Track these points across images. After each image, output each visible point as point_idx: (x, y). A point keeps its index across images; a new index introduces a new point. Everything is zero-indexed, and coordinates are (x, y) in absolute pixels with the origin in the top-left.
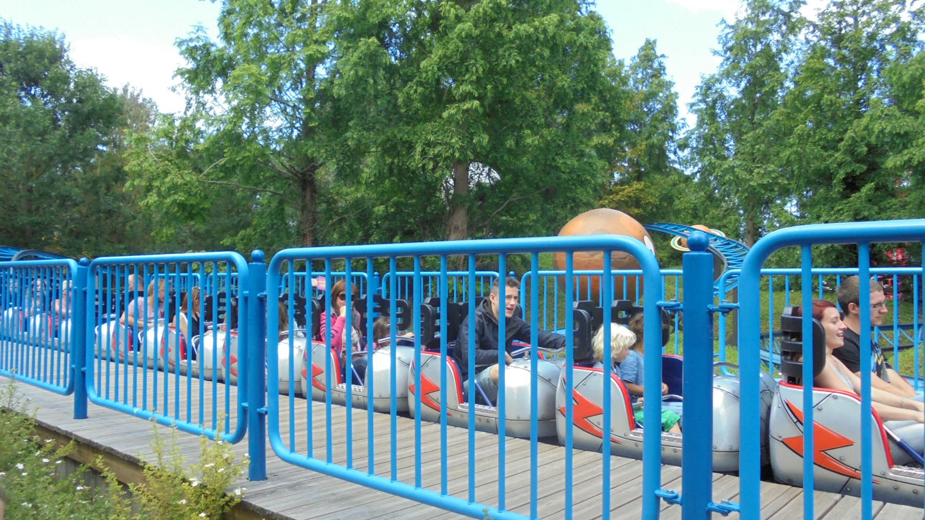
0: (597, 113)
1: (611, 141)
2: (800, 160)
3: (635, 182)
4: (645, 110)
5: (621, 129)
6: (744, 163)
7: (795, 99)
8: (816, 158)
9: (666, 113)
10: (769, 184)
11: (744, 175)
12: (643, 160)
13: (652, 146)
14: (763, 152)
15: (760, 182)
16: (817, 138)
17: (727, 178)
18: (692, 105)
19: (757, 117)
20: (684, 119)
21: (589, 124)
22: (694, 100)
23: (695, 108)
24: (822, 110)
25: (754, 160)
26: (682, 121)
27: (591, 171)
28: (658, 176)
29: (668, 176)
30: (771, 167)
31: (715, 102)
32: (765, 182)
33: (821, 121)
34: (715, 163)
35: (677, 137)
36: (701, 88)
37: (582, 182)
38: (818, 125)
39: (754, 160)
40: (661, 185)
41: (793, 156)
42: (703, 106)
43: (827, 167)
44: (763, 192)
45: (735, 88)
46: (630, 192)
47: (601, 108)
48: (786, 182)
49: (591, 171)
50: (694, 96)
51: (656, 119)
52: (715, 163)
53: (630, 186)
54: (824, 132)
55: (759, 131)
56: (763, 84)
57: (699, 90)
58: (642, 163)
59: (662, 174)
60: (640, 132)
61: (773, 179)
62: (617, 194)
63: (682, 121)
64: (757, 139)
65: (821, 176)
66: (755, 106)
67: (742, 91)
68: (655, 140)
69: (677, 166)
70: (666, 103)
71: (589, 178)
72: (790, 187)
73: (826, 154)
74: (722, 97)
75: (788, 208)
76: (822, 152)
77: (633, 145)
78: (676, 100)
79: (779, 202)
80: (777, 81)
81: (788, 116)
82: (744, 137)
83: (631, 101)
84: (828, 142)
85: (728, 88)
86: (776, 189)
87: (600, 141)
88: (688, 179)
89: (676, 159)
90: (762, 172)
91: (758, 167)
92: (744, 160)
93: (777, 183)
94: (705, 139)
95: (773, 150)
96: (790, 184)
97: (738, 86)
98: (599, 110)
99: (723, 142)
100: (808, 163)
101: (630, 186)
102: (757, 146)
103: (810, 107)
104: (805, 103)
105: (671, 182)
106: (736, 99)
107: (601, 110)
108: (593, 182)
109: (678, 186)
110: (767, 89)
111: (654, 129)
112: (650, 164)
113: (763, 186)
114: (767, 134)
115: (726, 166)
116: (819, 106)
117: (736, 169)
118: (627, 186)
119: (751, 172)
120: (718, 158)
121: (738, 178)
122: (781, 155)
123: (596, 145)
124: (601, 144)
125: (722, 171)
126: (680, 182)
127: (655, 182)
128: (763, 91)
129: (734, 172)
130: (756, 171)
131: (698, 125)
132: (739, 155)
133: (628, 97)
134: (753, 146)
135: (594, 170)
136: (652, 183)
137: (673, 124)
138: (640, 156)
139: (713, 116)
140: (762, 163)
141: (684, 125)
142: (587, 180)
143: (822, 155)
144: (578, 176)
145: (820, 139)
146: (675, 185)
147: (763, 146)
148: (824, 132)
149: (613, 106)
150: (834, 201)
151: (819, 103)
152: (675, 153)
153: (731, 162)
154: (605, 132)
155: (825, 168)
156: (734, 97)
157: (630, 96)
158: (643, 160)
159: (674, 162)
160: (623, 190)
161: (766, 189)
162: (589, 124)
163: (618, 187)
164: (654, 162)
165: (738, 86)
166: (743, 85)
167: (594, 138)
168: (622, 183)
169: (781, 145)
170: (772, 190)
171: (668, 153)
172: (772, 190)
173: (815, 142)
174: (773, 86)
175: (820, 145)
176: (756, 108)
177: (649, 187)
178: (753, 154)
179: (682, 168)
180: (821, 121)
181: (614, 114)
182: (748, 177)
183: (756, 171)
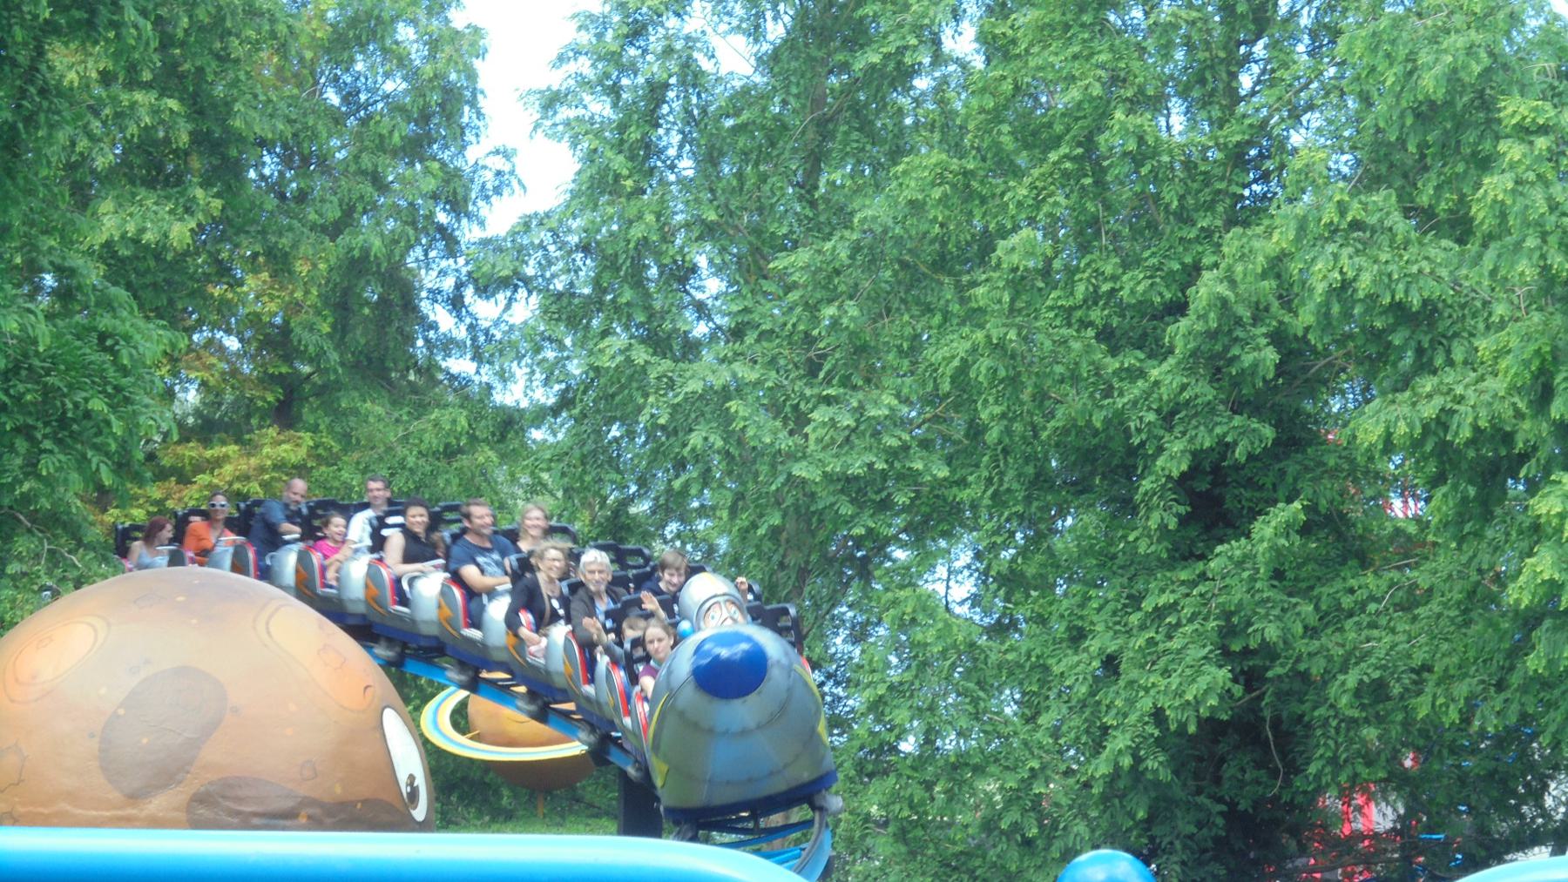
0: (125, 98)
1: (180, 233)
2: (1014, 381)
3: (272, 432)
4: (333, 97)
5: (226, 174)
6: (772, 378)
7: (996, 116)
8: (1074, 378)
9: (425, 117)
10: (875, 479)
11: (766, 431)
12: (311, 328)
13: (358, 265)
14: (853, 335)
15: (834, 466)
16: (1080, 290)
17: (695, 439)
18: (552, 101)
19: (835, 176)
20: (506, 154)
21: (83, 144)
22: (556, 80)
23: (565, 113)
24: (1099, 172)
25: (813, 369)
26: (498, 163)
27: (111, 372)
28: (375, 408)
29: (421, 409)
30: (883, 404)
31: (656, 91)
32: (857, 468)
33: (1095, 222)
34: (644, 370)
35: (469, 233)
36: (603, 23)
37: (63, 422)
38: (1087, 233)
39: (813, 369)
40: (389, 449)
41: (984, 364)
42: (600, 108)
43: (1118, 421)
44: (846, 509)
45: (740, 41)
46: (246, 478)
47: (147, 76)
48: (943, 472)
49: (111, 372)
50: (562, 59)
51: (381, 145)
52: (644, 370)
53: (250, 448)
54: (1109, 269)
55: (838, 247)
56: (858, 37)
57: (585, 38)
58: (310, 341)
59: (397, 395)
60: (302, 197)
61: (893, 455)
62: (184, 479)
63: (498, 163)
64: (827, 282)
65: (1088, 457)
66: (824, 127)
67: (775, 56)
68: (370, 235)
69: (461, 365)
70: (428, 70)
71: (98, 405)
72: (964, 495)
73: (1112, 364)
74: (692, 77)
75: (935, 583)
76: (1099, 353)
77: (279, 263)
78: (477, 64)
79: (900, 554)
80: (917, 29)
81: (966, 191)
82: (779, 263)
83: (282, 50)
84: (1122, 309)
85: (715, 41)
86: (901, 499)
87: (131, 228)
88: (509, 424)
89: (461, 333)
90: (847, 421)
91: (828, 400)
92: (772, 362)
93: (909, 477)
94: (609, 264)
95: (901, 325)
96: (962, 483)
97: (756, 32)
98: (133, 83)
99: (683, 274)
100: (1041, 396)
101: (250, 448)
102: (830, 311)
103: (1053, 156)
104: (1036, 138)
105: (431, 440)
106: (745, 91)
107: (148, 86)
108: (117, 427)
109: (464, 461)
110: (875, 59)
111: (368, 189)
112: (340, 345)
113: (847, 484)
114: (869, 254)
115: (695, 386)
116: (1089, 156)
117: (733, 405)
118: (232, 449)
119: (801, 420)
120: (659, 342)
121: (740, 442)
122: (934, 355)
123: (108, 245)
124: (136, 241)
125: (675, 408)
126: (473, 438)
127: (362, 432)
128: (859, 65)
129: (727, 418)
130: (820, 415)
131: (575, 195)
132: (750, 338)
133: (273, 35)
134: (812, 309)
135: (125, 371)
136: (346, 439)
137: (457, 173)
138: (296, 307)
139: (644, 154)
140: (846, 382)
141: (501, 185)
142: (88, 415)
143: (1097, 369)
144: (48, 392)
145: (1093, 298)
146: (450, 453)
147: (852, 310)
148: (1109, 269)
149: (200, 71)
150: (1140, 568)
151: (1089, 142)
152: (456, 303)
153: (705, 373)
154: (150, 184)
155: (1107, 422)
156: (738, 84)
157: (281, 29)
158: (311, 328)
159: (448, 345)
160: (218, 463)
161: (858, 502)
162: (83, 144)
163: (192, 451)
164: (360, 337)
165: (756, 32)
166: (775, 31)
167: (106, 206)
168: (206, 428)
169: (928, 310)
170: (885, 505)
171: (425, 306)
172: (885, 505)
173: (1072, 309)
174: (902, 50)
175: (1091, 324)
176: (826, 136)
177: (332, 460)
178: (809, 340)
179: (487, 375)
180: (1095, 222)
181: (199, 106)
182: (786, 442)
183: (820, 415)
